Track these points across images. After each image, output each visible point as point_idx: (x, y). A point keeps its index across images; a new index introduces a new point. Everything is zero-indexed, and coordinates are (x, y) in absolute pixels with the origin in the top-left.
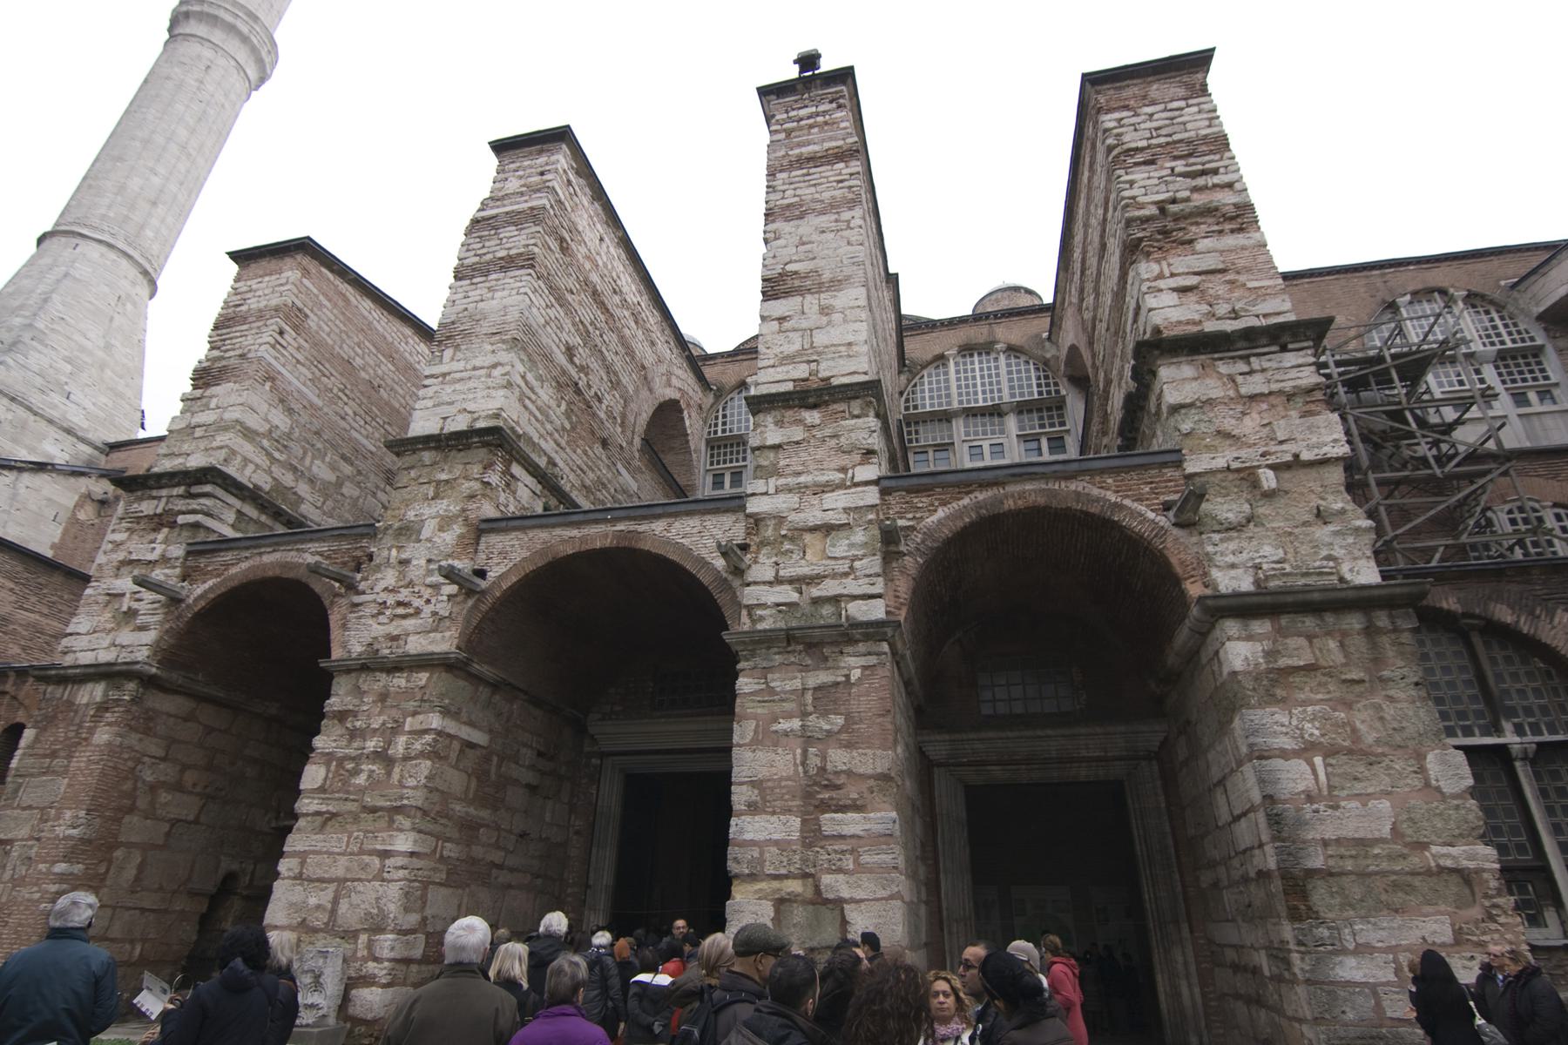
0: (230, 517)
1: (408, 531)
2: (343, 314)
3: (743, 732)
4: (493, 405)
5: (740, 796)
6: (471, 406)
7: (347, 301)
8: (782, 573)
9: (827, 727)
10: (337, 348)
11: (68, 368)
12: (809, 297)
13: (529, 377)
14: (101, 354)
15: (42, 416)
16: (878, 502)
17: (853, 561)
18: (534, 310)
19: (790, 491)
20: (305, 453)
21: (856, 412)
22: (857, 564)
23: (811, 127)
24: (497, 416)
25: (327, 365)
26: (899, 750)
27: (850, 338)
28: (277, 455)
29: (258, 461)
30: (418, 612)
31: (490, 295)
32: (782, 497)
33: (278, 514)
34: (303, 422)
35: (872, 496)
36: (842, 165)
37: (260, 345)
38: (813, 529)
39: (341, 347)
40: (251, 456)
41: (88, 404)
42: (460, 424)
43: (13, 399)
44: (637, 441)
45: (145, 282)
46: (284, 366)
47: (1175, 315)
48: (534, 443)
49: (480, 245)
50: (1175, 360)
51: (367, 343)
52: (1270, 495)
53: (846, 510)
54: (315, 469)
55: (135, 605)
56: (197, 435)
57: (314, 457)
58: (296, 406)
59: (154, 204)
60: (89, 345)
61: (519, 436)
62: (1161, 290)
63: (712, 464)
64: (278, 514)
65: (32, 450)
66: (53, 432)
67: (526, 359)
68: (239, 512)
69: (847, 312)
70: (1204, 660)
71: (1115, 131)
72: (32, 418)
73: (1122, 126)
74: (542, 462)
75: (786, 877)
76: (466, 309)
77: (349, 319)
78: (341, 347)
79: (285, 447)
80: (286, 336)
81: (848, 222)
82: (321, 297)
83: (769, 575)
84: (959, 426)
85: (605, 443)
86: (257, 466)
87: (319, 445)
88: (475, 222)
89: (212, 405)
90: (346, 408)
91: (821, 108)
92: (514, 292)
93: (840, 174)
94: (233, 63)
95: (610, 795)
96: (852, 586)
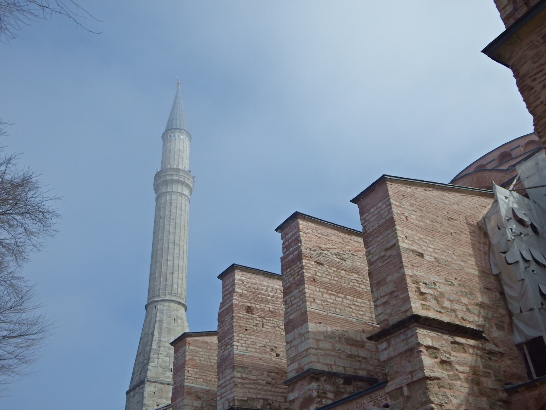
2: (207, 349)
6: (228, 397)
7: (207, 343)
10: (209, 363)
23: (291, 242)
25: (207, 372)
34: (205, 399)
39: (210, 362)
43: (155, 382)
45: (181, 307)
46: (192, 383)
48: (254, 399)
50: (381, 341)
52: (408, 397)
58: (201, 395)
59: (173, 273)
61: (246, 401)
72: (163, 386)
77: (210, 349)
78: (210, 362)
80: (190, 372)
82: (198, 349)
88: (219, 315)
91: (294, 232)
93: (298, 268)
94: (178, 194)
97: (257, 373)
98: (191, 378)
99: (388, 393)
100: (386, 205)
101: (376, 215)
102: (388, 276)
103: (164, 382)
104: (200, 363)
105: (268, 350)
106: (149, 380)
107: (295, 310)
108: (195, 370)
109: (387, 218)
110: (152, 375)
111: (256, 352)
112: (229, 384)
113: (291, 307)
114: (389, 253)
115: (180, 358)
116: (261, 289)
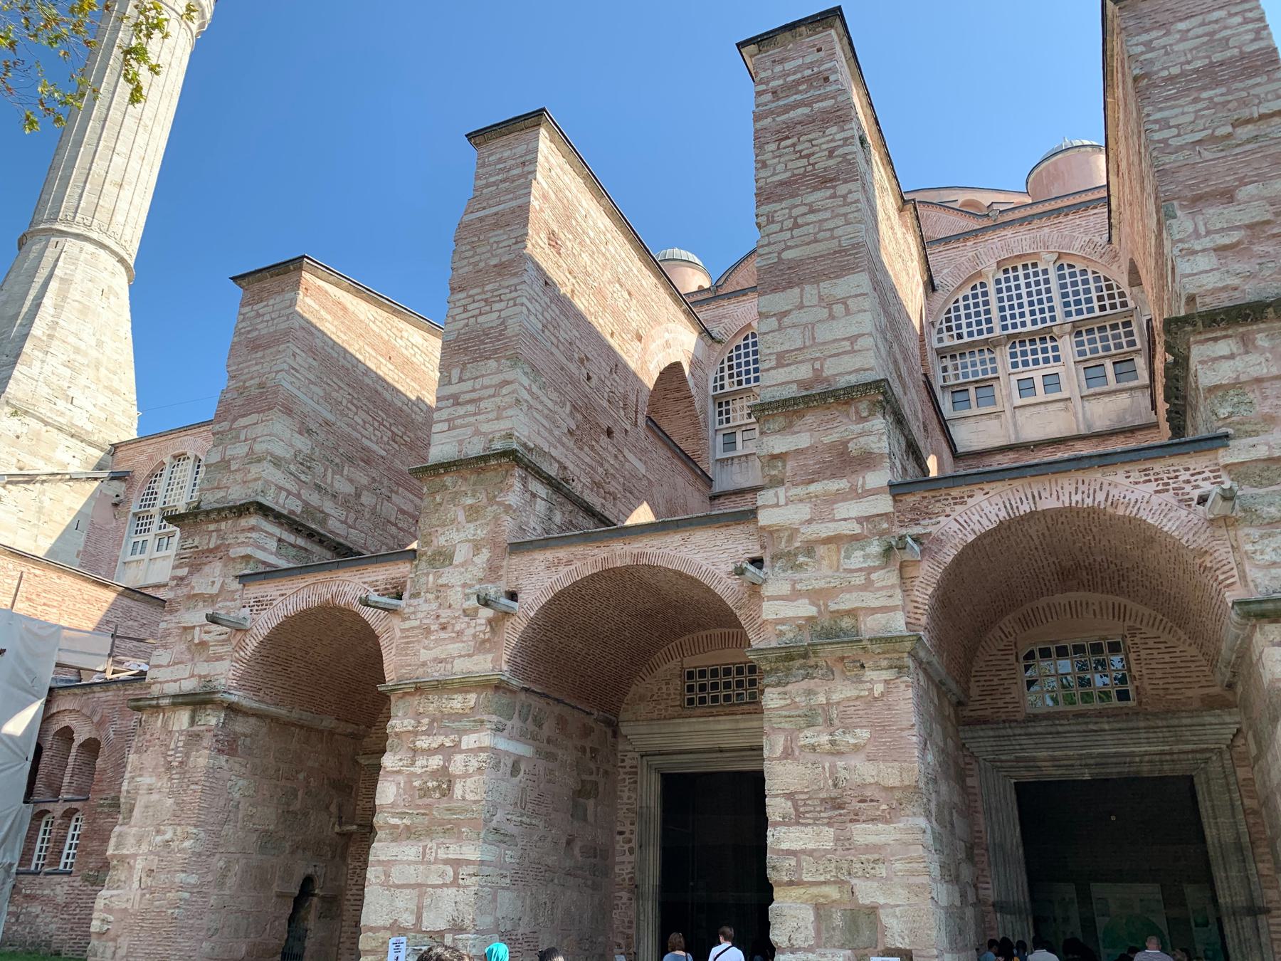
0: (273, 545)
1: (443, 558)
2: (343, 323)
3: (774, 746)
4: (504, 425)
5: (775, 807)
7: (344, 309)
8: (798, 587)
9: (852, 741)
11: (68, 372)
12: (807, 288)
13: (534, 389)
14: (94, 353)
15: (53, 426)
16: (892, 510)
17: (869, 574)
18: (532, 318)
19: (801, 501)
20: (326, 471)
21: (865, 414)
22: (874, 576)
24: (510, 436)
26: (930, 758)
27: (853, 330)
28: (303, 477)
29: (288, 486)
30: (460, 633)
31: (488, 308)
32: (792, 508)
33: (311, 535)
35: (885, 504)
36: (834, 129)
37: (277, 372)
38: (828, 541)
40: (282, 483)
41: (91, 408)
42: (475, 448)
44: (642, 420)
46: (299, 389)
47: (1211, 281)
49: (471, 253)
51: (366, 347)
53: (860, 520)
54: (336, 485)
55: (206, 637)
56: (233, 467)
57: (334, 473)
58: (313, 427)
60: (83, 346)
61: (530, 450)
62: (1196, 252)
63: (721, 422)
64: (311, 535)
65: (48, 460)
66: (63, 439)
67: (529, 370)
68: (280, 540)
69: (849, 302)
70: (1255, 659)
71: (1142, 58)
73: (1153, 50)
74: (552, 471)
75: (825, 883)
76: (467, 325)
79: (309, 468)
81: (845, 197)
83: (786, 589)
84: (1003, 356)
85: (609, 433)
86: (289, 493)
87: (337, 460)
89: (243, 438)
90: (356, 418)
91: (808, 60)
92: (511, 303)
95: (649, 794)
96: (872, 600)
97: (554, 396)
98: (297, 375)
99: (1225, 466)
100: (1245, 19)
101: (1198, 37)
102: (1246, 184)
103: (50, 421)
104: (323, 349)
105: (576, 356)
106: (10, 401)
107: (807, 239)
108: (310, 360)
109: (1248, 49)
110: (20, 395)
111: (557, 347)
112: (490, 396)
113: (791, 229)
114: (1245, 132)
115: (267, 317)
116: (579, 212)
